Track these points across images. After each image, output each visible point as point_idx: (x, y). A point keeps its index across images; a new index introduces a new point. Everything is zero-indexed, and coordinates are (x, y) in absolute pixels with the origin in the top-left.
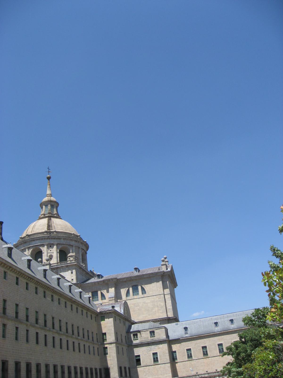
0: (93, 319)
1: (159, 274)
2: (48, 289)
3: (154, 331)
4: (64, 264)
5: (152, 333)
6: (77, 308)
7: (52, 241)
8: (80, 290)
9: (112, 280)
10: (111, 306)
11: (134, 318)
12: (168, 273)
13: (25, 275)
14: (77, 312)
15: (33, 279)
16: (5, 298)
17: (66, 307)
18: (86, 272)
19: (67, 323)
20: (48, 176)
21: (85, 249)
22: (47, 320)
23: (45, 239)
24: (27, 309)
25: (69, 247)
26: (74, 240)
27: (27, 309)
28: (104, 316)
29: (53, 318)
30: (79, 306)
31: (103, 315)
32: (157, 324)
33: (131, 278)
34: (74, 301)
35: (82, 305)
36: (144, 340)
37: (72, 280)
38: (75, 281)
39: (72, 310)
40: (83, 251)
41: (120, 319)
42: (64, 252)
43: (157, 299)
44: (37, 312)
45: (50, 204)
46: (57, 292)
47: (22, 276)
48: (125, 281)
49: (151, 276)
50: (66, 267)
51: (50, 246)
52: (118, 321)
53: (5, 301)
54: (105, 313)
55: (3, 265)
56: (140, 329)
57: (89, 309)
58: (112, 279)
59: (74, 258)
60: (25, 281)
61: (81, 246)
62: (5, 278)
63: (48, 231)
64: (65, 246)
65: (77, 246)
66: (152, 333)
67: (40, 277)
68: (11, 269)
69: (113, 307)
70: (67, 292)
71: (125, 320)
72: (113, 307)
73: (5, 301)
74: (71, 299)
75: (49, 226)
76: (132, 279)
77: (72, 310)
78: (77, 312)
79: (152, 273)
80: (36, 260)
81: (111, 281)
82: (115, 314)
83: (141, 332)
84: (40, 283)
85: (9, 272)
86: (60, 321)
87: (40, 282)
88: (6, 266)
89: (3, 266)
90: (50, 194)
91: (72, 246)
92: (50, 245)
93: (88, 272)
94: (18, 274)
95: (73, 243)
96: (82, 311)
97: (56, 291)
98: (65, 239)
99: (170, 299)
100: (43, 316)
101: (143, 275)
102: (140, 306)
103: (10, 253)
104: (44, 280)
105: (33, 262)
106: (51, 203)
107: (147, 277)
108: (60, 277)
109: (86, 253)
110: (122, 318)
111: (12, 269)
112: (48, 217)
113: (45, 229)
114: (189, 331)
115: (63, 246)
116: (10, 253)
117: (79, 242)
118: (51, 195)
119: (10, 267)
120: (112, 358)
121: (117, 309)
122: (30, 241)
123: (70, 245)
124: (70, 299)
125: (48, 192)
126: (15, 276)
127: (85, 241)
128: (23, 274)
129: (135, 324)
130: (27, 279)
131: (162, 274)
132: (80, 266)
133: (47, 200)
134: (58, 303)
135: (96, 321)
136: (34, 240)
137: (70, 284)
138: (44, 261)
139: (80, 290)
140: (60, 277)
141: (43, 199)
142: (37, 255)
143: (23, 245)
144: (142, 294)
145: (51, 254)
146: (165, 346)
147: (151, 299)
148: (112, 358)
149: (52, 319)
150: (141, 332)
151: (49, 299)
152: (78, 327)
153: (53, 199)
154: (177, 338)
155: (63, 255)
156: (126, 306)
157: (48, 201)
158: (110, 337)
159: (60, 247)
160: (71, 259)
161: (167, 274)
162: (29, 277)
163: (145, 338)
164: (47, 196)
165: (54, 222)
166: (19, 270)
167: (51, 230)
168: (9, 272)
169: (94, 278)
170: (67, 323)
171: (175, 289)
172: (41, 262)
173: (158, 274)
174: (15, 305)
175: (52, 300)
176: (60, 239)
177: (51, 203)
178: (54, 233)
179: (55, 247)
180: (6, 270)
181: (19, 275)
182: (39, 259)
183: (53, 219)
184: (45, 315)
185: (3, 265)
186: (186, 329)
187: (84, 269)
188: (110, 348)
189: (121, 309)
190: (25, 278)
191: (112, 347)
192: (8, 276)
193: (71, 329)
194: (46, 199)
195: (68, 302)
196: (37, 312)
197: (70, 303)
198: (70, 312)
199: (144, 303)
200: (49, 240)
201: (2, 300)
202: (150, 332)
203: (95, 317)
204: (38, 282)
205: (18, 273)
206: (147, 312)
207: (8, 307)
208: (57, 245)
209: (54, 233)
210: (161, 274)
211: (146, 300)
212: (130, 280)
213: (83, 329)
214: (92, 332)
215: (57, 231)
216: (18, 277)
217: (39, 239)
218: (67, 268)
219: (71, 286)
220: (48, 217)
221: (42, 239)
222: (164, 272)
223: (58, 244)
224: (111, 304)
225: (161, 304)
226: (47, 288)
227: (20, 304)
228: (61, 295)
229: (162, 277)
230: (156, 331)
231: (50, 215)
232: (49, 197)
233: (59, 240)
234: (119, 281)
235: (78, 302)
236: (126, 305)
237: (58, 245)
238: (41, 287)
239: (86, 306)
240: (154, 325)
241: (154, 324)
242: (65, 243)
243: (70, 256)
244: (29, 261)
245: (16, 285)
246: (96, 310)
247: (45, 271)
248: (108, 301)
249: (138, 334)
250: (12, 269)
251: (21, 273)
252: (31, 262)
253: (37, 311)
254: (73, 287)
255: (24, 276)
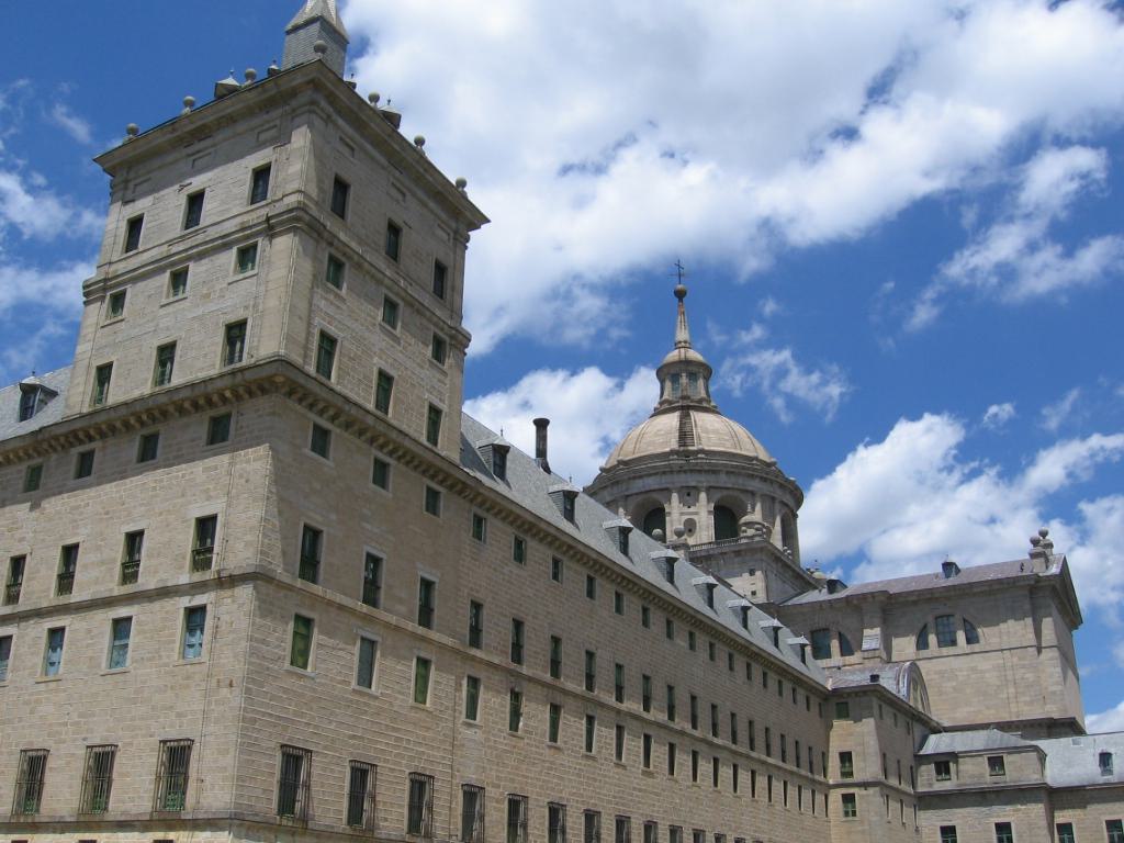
0: (812, 709)
1: (1022, 583)
2: (680, 614)
3: (1002, 757)
4: (728, 546)
5: (996, 763)
6: (765, 674)
7: (692, 480)
8: (776, 623)
9: (873, 597)
10: (868, 675)
11: (939, 713)
12: (1053, 582)
13: (613, 572)
14: (765, 685)
15: (635, 584)
16: (557, 633)
17: (731, 668)
18: (794, 571)
19: (733, 715)
20: (680, 287)
21: (791, 503)
22: (677, 702)
23: (672, 472)
24: (619, 667)
25: (743, 497)
26: (757, 476)
27: (619, 667)
28: (847, 703)
29: (693, 698)
30: (769, 668)
31: (842, 703)
32: (1013, 739)
33: (932, 594)
34: (756, 654)
35: (779, 667)
36: (969, 781)
37: (754, 593)
38: (761, 598)
39: (749, 677)
40: (785, 510)
41: (895, 715)
42: (730, 510)
43: (1015, 659)
44: (646, 678)
45: (686, 371)
46: (705, 624)
47: (602, 574)
48: (915, 603)
49: (996, 587)
50: (736, 556)
51: (689, 495)
52: (889, 721)
53: (556, 641)
54: (849, 694)
55: (549, 539)
56: (958, 748)
57: (800, 679)
58: (873, 594)
59: (757, 530)
60: (612, 588)
61: (779, 494)
62: (555, 577)
63: (682, 448)
64: (731, 492)
65: (766, 495)
66: (996, 763)
67: (655, 577)
68: (571, 552)
69: (875, 678)
70: (734, 624)
71: (912, 719)
72: (875, 678)
73: (556, 641)
74: (747, 648)
75: (684, 435)
76: (937, 595)
77: (749, 677)
78: (765, 685)
79: (999, 581)
80: (648, 531)
81: (871, 600)
82: (879, 698)
83: (960, 760)
84: (655, 596)
85: (566, 562)
86: (714, 707)
87: (657, 593)
88: (557, 543)
89: (550, 544)
90: (685, 342)
91: (753, 493)
92: (685, 491)
93: (801, 573)
94: (591, 567)
95: (755, 485)
96: (780, 682)
97: (701, 622)
98: (732, 473)
99: (1059, 661)
100: (666, 690)
101: (969, 584)
102: (960, 678)
103: (568, 507)
104: (667, 587)
105: (637, 537)
106: (690, 368)
107: (982, 592)
108: (715, 582)
109: (795, 516)
110: (899, 711)
111: (576, 553)
112: (682, 408)
113: (674, 444)
114: (1116, 763)
115: (725, 493)
116: (568, 507)
117: (772, 482)
118: (688, 345)
119: (570, 547)
120: (867, 827)
121: (887, 682)
122: (630, 479)
123: (747, 491)
124: (742, 646)
125: (682, 335)
126: (585, 572)
127: (792, 479)
128: (608, 568)
129: (940, 732)
130: (619, 584)
131: (1032, 582)
132: (779, 555)
133: (676, 358)
134: (706, 656)
135: (821, 716)
136: (641, 477)
137: (745, 603)
138: (671, 537)
139: (776, 623)
140: (715, 582)
141: (664, 356)
142: (651, 518)
143: (609, 489)
144: (969, 641)
145: (694, 518)
146: (1037, 810)
147: (995, 659)
148: (867, 827)
149: (689, 701)
150: (960, 760)
151: (682, 642)
152: (767, 730)
153: (694, 355)
154: (1077, 784)
155: (727, 519)
156: (915, 678)
157: (680, 362)
158: (862, 764)
159: (718, 495)
160: (751, 532)
161: (1047, 583)
162: (624, 578)
163: (972, 776)
164: (677, 345)
165: (699, 423)
166: (594, 556)
167: (691, 448)
168: (566, 562)
169: (817, 591)
170: (733, 715)
171: (1074, 632)
172: (662, 539)
173: (1018, 584)
174: (584, 654)
175: (692, 647)
176: (714, 472)
177: (690, 368)
178: (699, 456)
179: (703, 496)
180: (559, 556)
181: (596, 571)
182: (657, 531)
183: (696, 416)
184: (670, 688)
185: (549, 539)
186: (1105, 759)
187: (789, 563)
188: (862, 797)
189: (898, 684)
190: (613, 581)
191: (868, 795)
192: (565, 573)
193: (747, 734)
194: (673, 356)
195: (736, 656)
196: (646, 678)
197: (745, 659)
198: (744, 683)
199: (974, 669)
200: (683, 476)
201: (548, 636)
202: (989, 759)
203: (820, 704)
204: (650, 593)
205: (591, 563)
206: (982, 698)
207: (564, 659)
208: (709, 489)
209: (699, 456)
210: (1027, 582)
211: (984, 664)
212: (930, 599)
213: (782, 736)
214: (810, 749)
215: (706, 448)
216: (592, 575)
217: (656, 474)
218: (736, 560)
219: (749, 608)
220: (682, 408)
221: (664, 473)
222: (1038, 579)
223: (711, 487)
224: (872, 669)
225: (1027, 676)
226: (675, 612)
227: (599, 653)
228: (717, 634)
229: (1031, 593)
230: (1007, 759)
231: (686, 403)
232: (682, 350)
233: (713, 476)
234: (893, 601)
235: (767, 657)
236: (914, 675)
237: (712, 490)
238: (660, 607)
239: (790, 670)
240: (1001, 740)
241: (1002, 736)
242: (730, 486)
243: (746, 524)
244: (625, 532)
245: (588, 599)
246: (822, 683)
247: (671, 561)
248: (861, 661)
249: (952, 766)
250: (576, 553)
251: (602, 565)
252: (631, 535)
253: (647, 673)
254: (754, 613)
255: (609, 573)
